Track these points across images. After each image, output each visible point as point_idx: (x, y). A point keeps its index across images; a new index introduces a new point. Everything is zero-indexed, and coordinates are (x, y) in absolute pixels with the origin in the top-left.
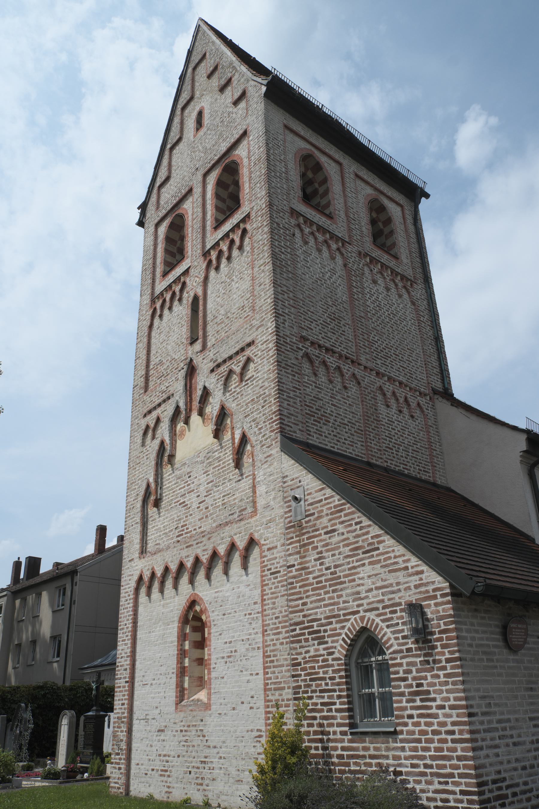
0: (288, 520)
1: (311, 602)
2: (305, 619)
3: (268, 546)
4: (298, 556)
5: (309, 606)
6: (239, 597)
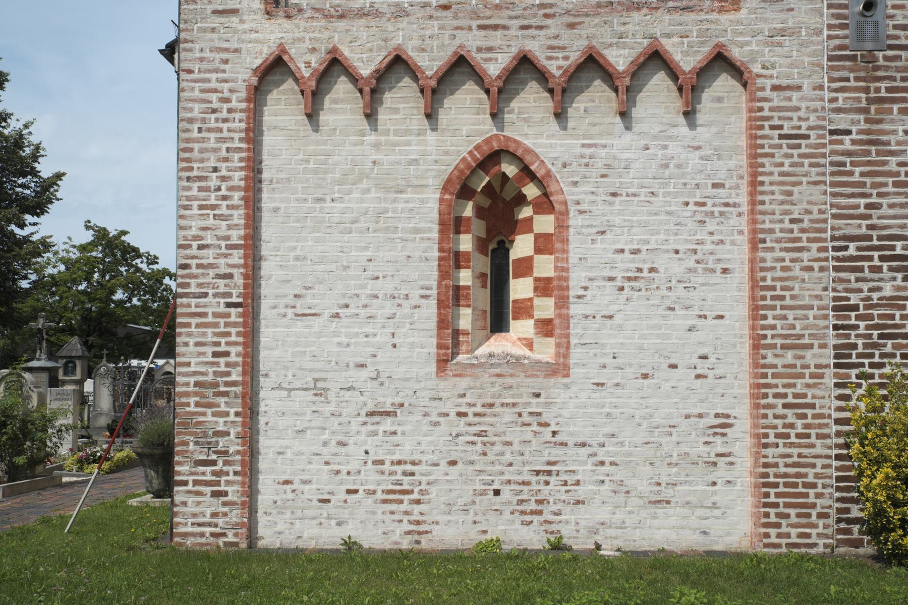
0: (837, 42)
1: (891, 206)
2: (875, 233)
3: (776, 82)
4: (862, 117)
5: (885, 211)
6: (666, 166)
